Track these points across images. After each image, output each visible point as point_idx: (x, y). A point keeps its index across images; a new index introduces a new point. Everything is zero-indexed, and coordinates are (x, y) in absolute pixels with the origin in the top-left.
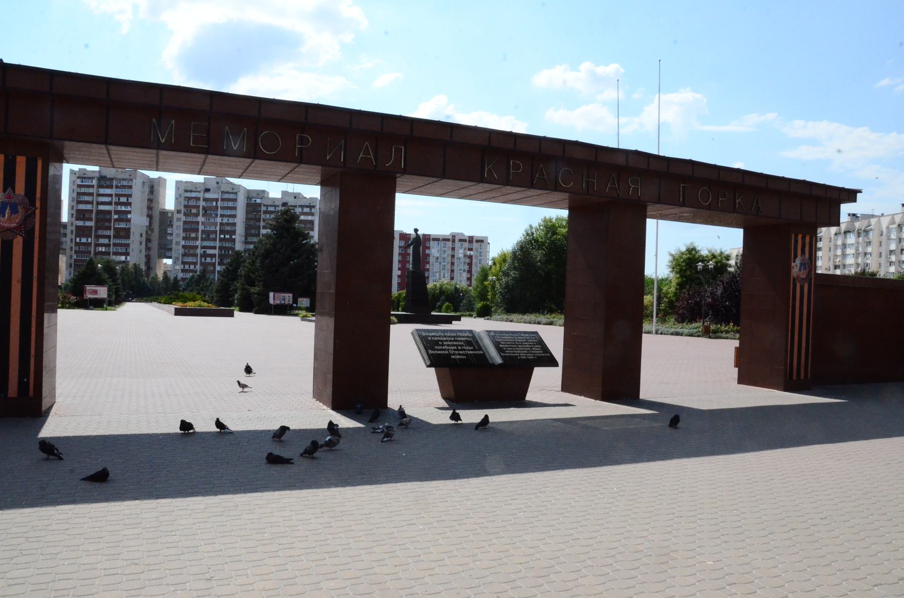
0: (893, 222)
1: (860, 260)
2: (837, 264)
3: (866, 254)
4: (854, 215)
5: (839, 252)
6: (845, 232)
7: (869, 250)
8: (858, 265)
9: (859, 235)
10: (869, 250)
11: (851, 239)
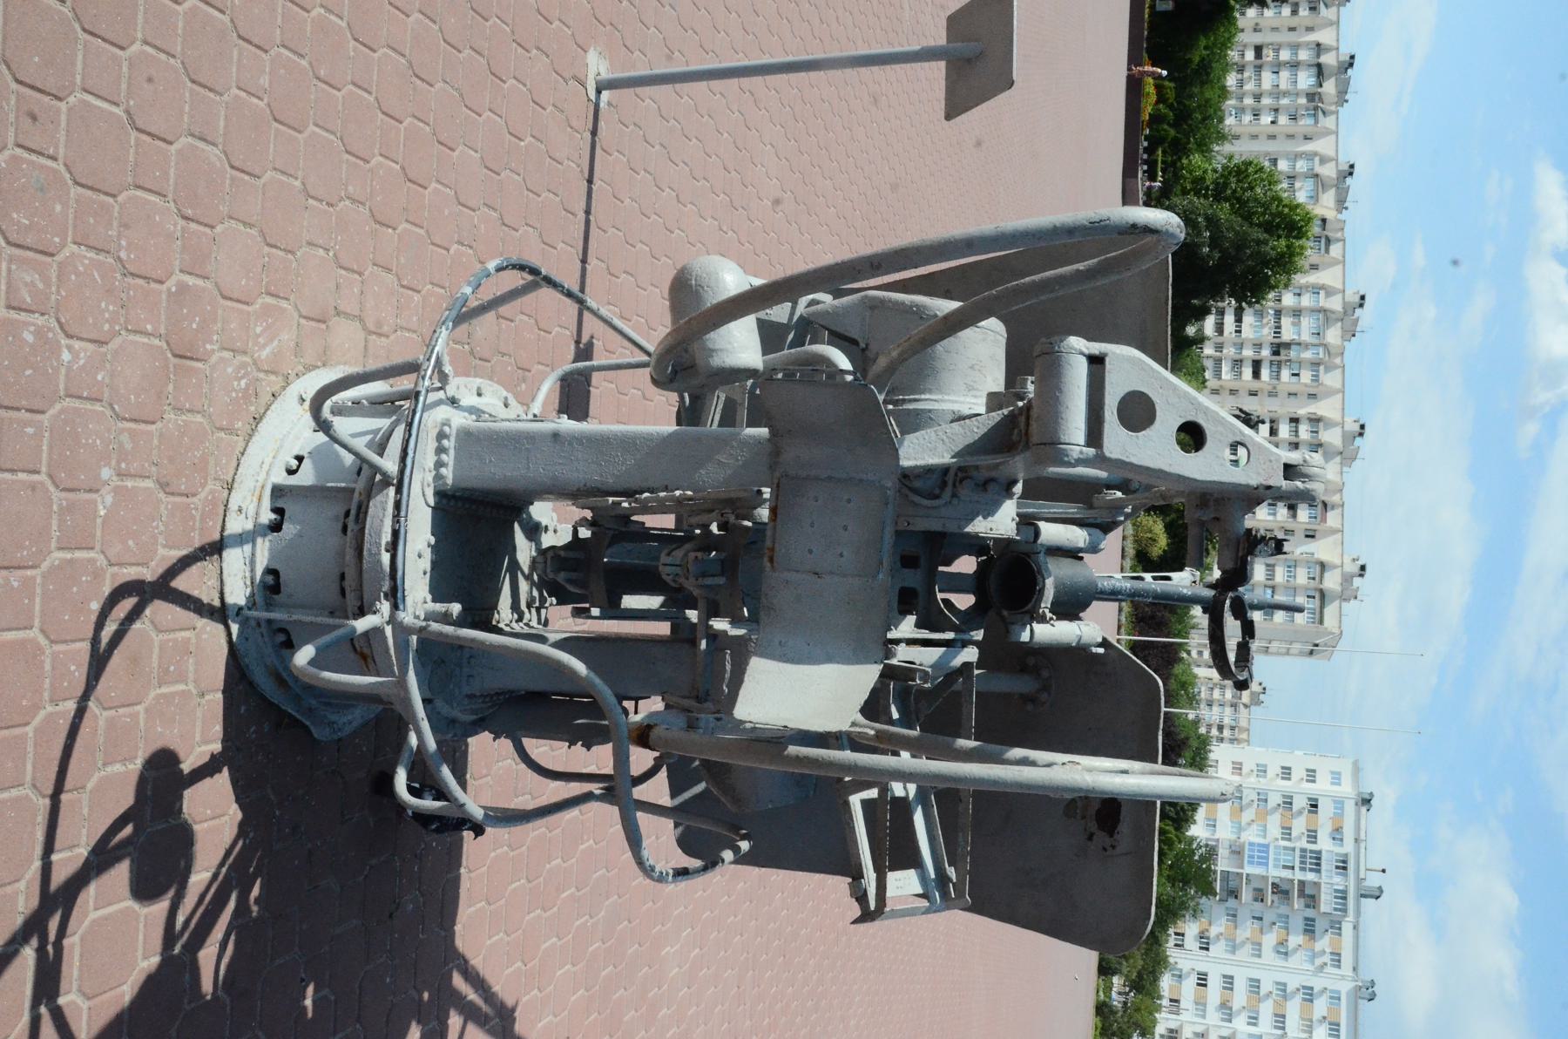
0: (1323, 160)
1: (1266, 101)
2: (1265, 52)
3: (1276, 110)
4: (1351, 65)
5: (1285, 55)
6: (1319, 66)
7: (1283, 120)
8: (1257, 97)
9: (1311, 96)
10: (1283, 120)
11: (1306, 80)
